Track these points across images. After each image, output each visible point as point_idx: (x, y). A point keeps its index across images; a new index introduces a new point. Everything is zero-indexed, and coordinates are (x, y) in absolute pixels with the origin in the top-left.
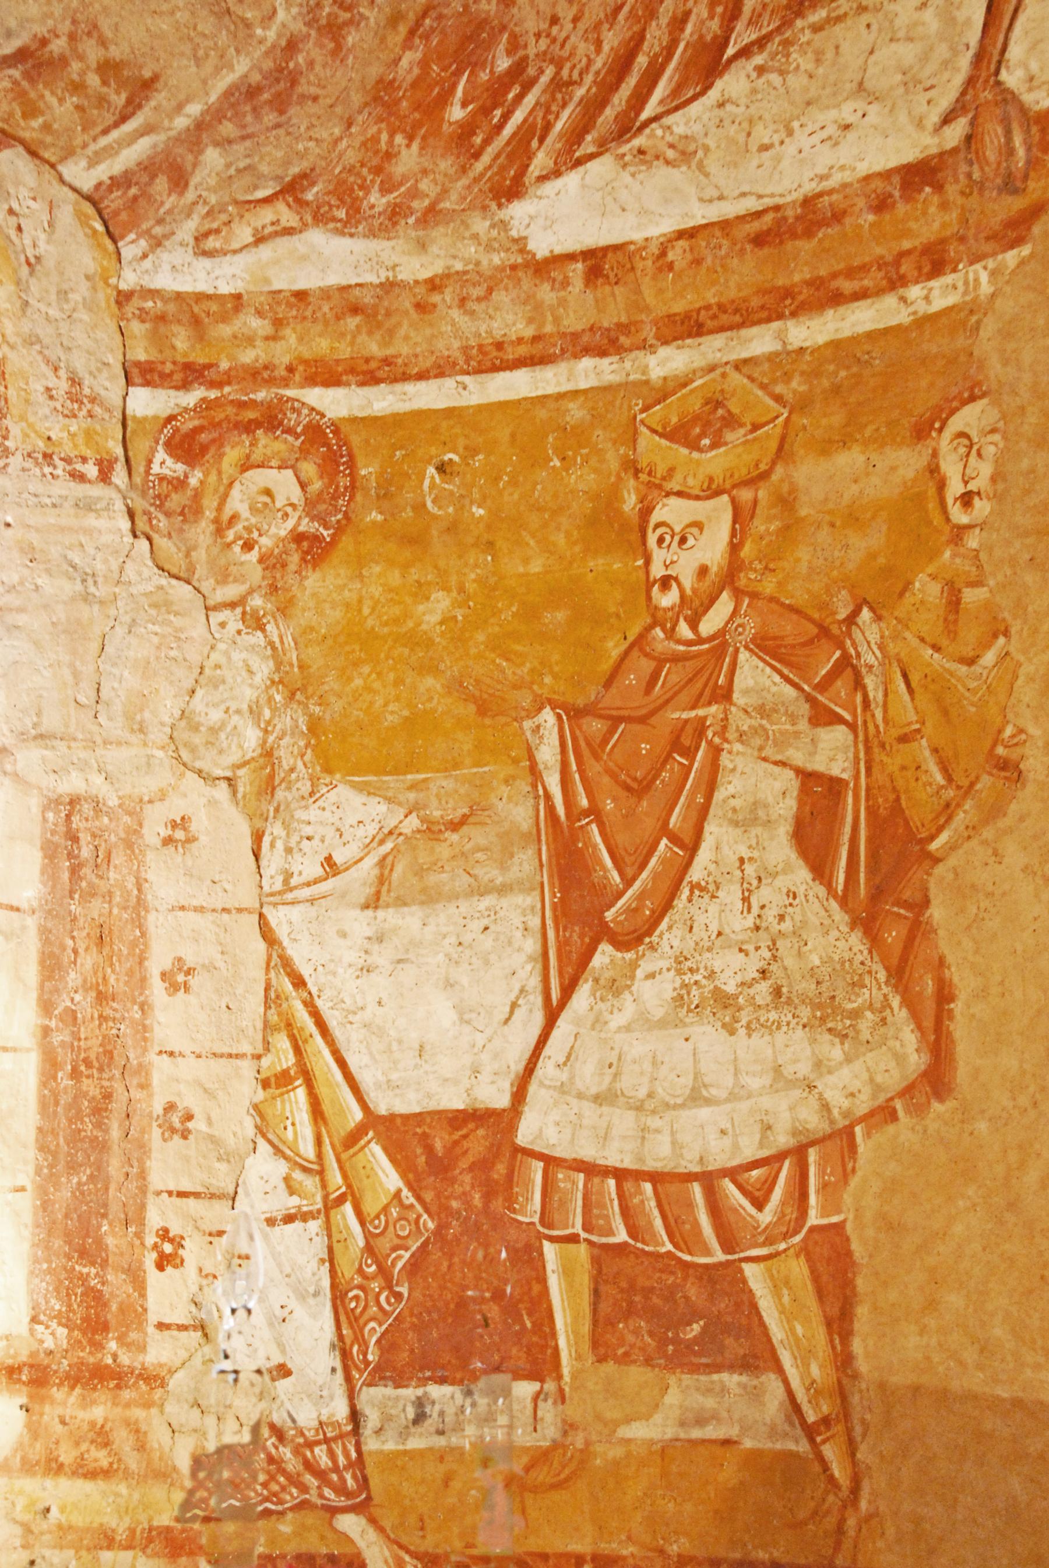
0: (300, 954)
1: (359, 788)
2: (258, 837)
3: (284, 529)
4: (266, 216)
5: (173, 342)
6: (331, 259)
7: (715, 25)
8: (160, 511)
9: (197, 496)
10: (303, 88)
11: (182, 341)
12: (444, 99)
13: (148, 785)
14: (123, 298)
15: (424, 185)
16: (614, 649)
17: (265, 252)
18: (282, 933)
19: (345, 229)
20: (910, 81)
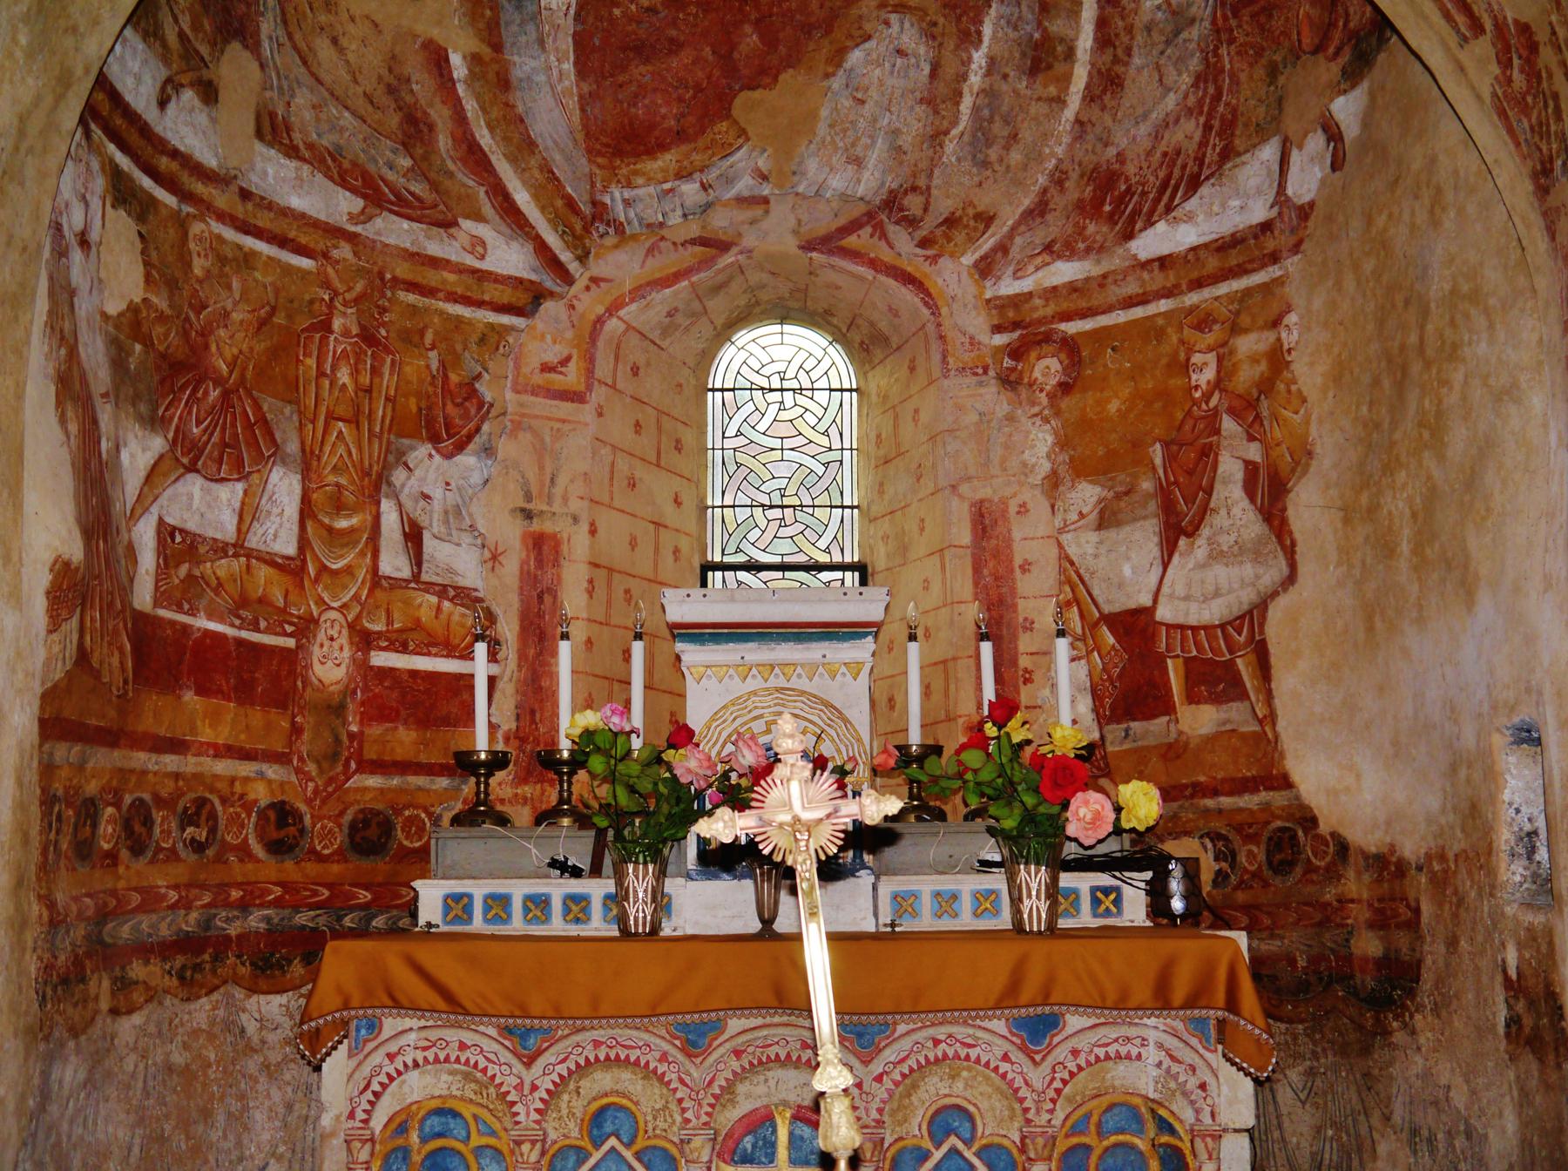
0: (1072, 551)
1: (1091, 482)
2: (1053, 507)
3: (1054, 382)
4: (1039, 260)
5: (1009, 314)
6: (1065, 272)
7: (1196, 169)
8: (1009, 381)
9: (1021, 372)
10: (1052, 206)
11: (1011, 314)
12: (1102, 204)
13: (1008, 492)
14: (988, 301)
15: (1098, 238)
16: (1179, 415)
17: (1040, 274)
18: (1065, 543)
19: (1069, 259)
20: (1259, 192)
